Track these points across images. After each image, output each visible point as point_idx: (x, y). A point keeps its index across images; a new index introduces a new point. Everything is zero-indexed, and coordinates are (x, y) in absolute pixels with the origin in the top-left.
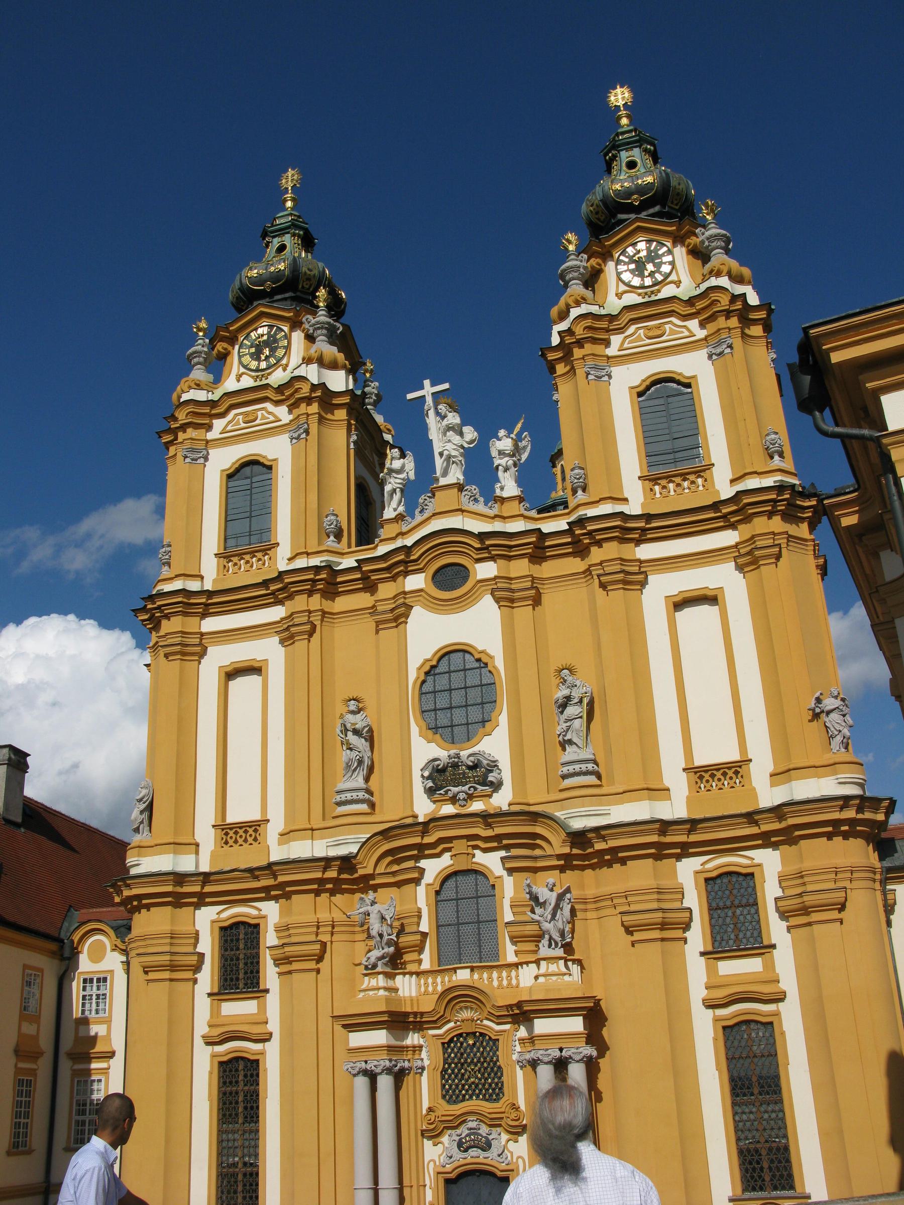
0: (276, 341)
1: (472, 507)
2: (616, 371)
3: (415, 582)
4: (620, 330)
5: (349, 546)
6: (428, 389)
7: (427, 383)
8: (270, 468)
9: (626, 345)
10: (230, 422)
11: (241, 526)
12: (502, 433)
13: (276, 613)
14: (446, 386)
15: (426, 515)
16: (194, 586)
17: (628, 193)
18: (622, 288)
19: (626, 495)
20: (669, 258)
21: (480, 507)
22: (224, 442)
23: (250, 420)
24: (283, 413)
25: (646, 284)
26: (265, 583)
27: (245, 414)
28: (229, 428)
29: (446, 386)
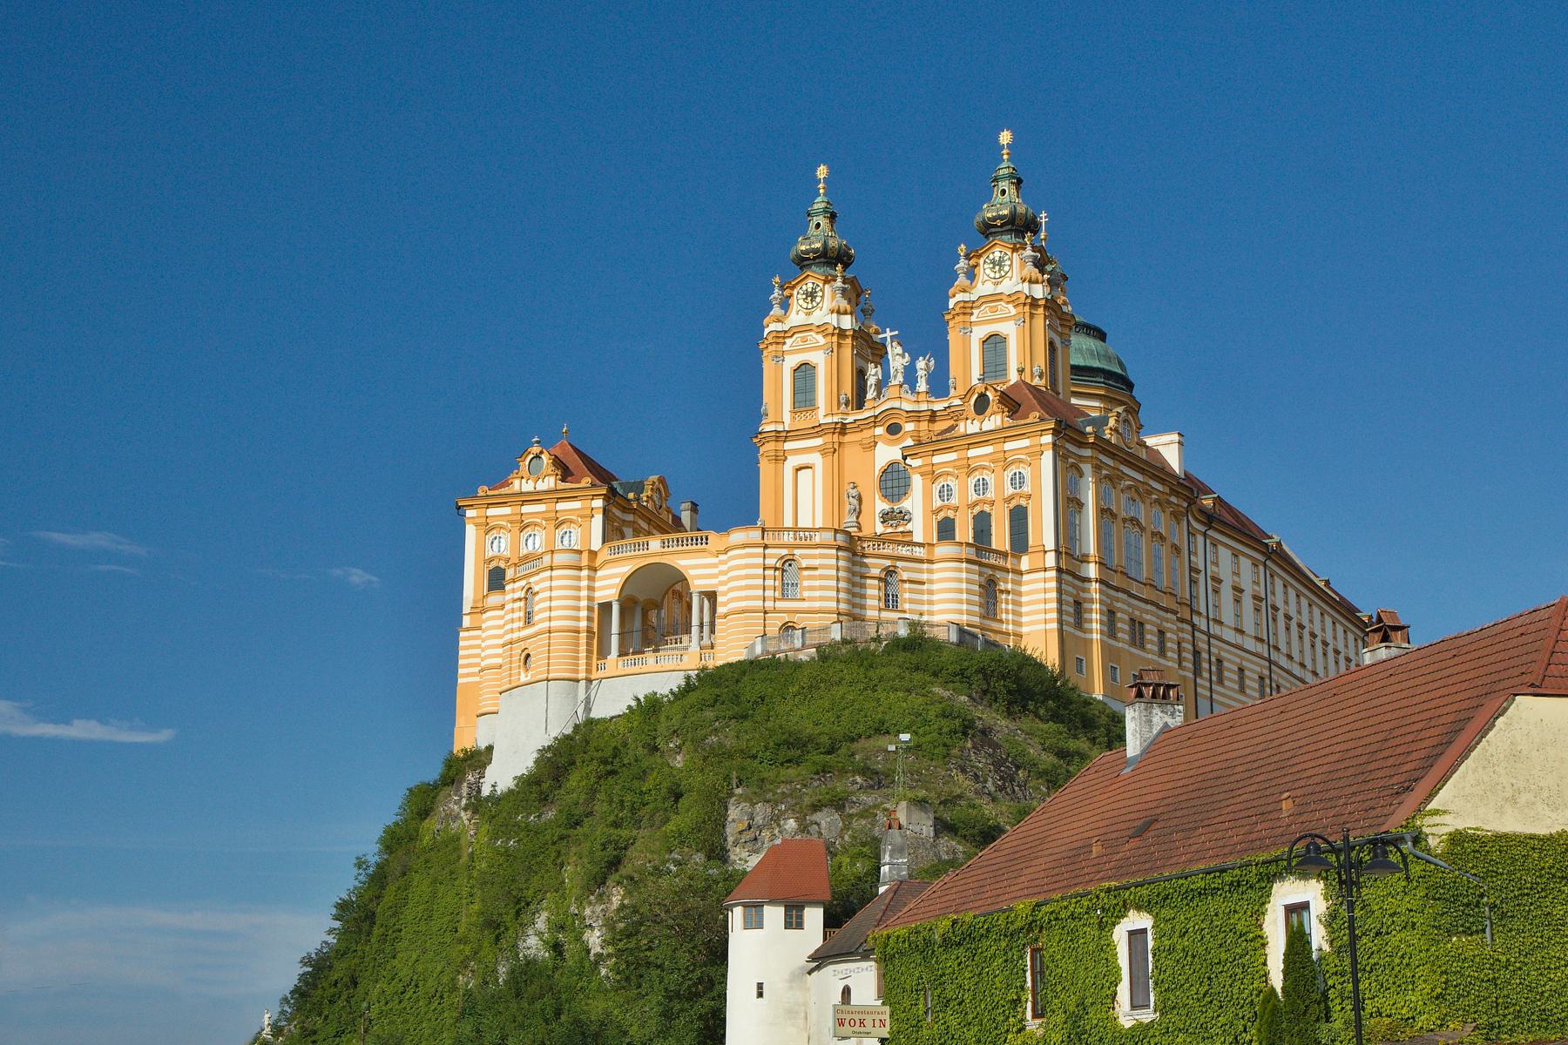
0: (816, 292)
3: (880, 431)
5: (852, 410)
6: (888, 334)
7: (888, 330)
12: (921, 358)
13: (818, 441)
14: (897, 333)
15: (885, 399)
16: (780, 428)
17: (994, 219)
21: (909, 396)
22: (791, 352)
23: (804, 340)
24: (821, 340)
26: (813, 428)
29: (897, 333)
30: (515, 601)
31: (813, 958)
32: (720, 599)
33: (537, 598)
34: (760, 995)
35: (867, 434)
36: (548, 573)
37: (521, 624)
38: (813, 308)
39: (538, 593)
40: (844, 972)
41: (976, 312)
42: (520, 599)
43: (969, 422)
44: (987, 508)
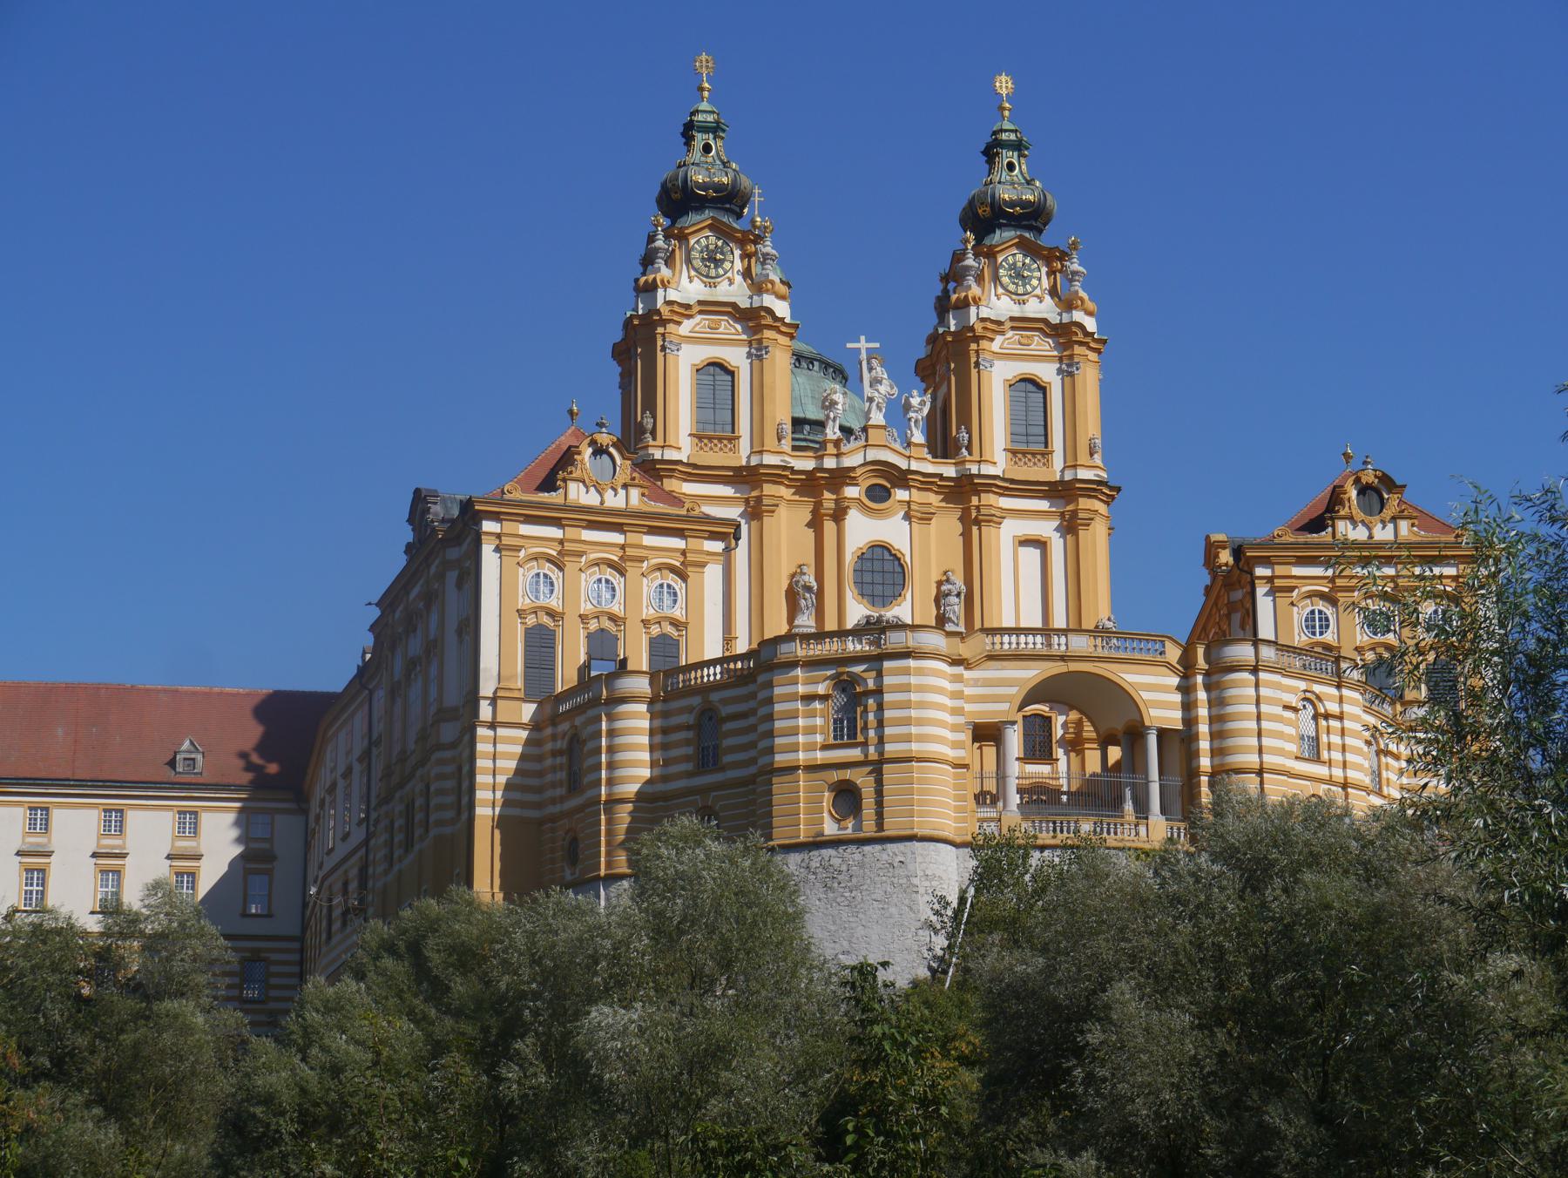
1: (894, 445)
2: (997, 363)
3: (851, 492)
4: (1002, 333)
6: (863, 344)
7: (863, 338)
8: (731, 373)
9: (1005, 345)
10: (698, 324)
11: (709, 414)
17: (1012, 204)
18: (1000, 290)
19: (995, 460)
21: (897, 446)
25: (1019, 292)
26: (741, 468)
28: (697, 329)
38: (718, 276)
41: (999, 339)
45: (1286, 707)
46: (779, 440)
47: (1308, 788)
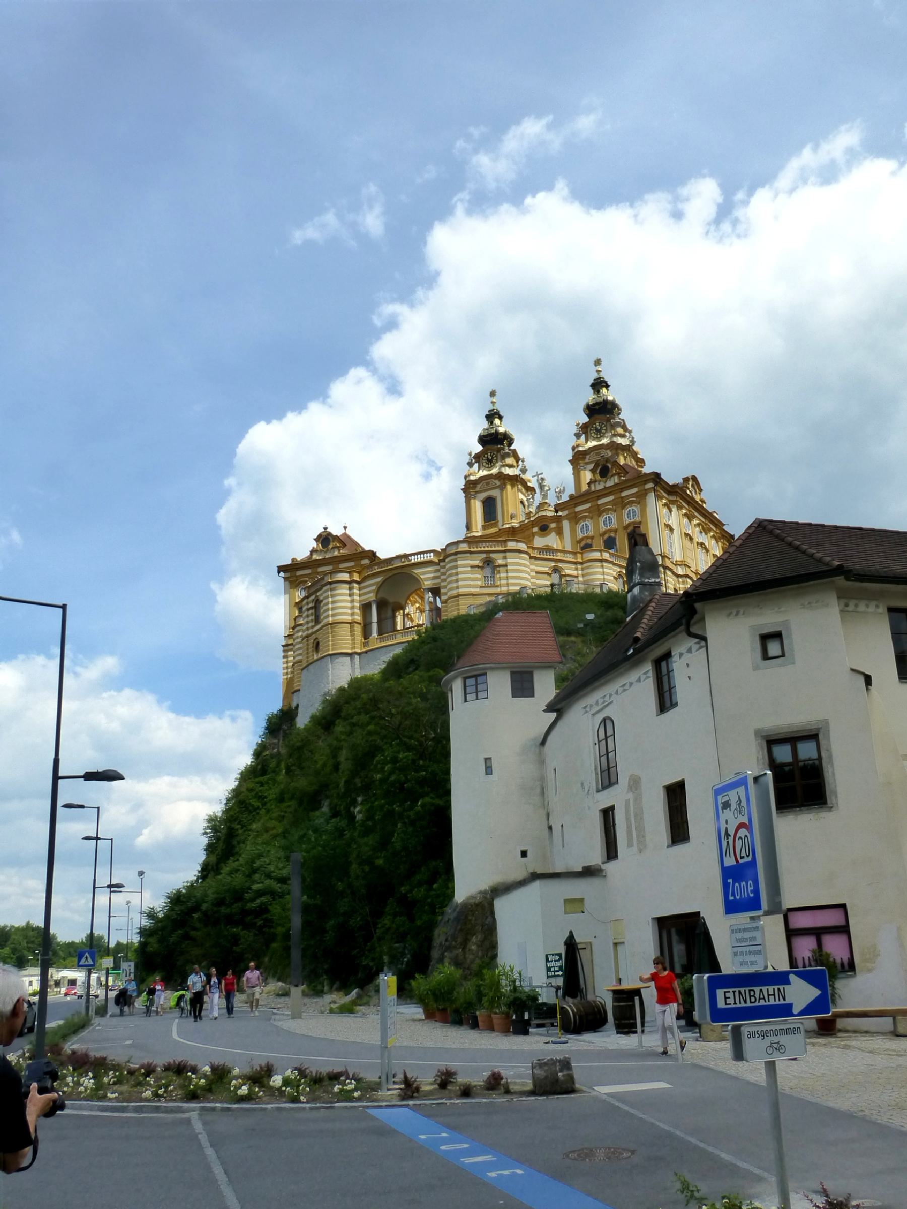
3: (536, 529)
20: (605, 428)
23: (488, 484)
27: (487, 483)
30: (308, 610)
31: (550, 708)
32: (443, 591)
33: (322, 604)
34: (489, 770)
35: (527, 533)
36: (328, 587)
37: (313, 624)
39: (322, 601)
40: (601, 701)
41: (588, 457)
42: (311, 608)
43: (597, 483)
44: (612, 534)
45: (472, 567)
46: (511, 518)
47: (488, 599)
